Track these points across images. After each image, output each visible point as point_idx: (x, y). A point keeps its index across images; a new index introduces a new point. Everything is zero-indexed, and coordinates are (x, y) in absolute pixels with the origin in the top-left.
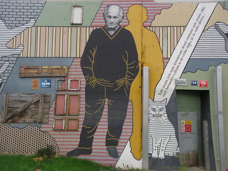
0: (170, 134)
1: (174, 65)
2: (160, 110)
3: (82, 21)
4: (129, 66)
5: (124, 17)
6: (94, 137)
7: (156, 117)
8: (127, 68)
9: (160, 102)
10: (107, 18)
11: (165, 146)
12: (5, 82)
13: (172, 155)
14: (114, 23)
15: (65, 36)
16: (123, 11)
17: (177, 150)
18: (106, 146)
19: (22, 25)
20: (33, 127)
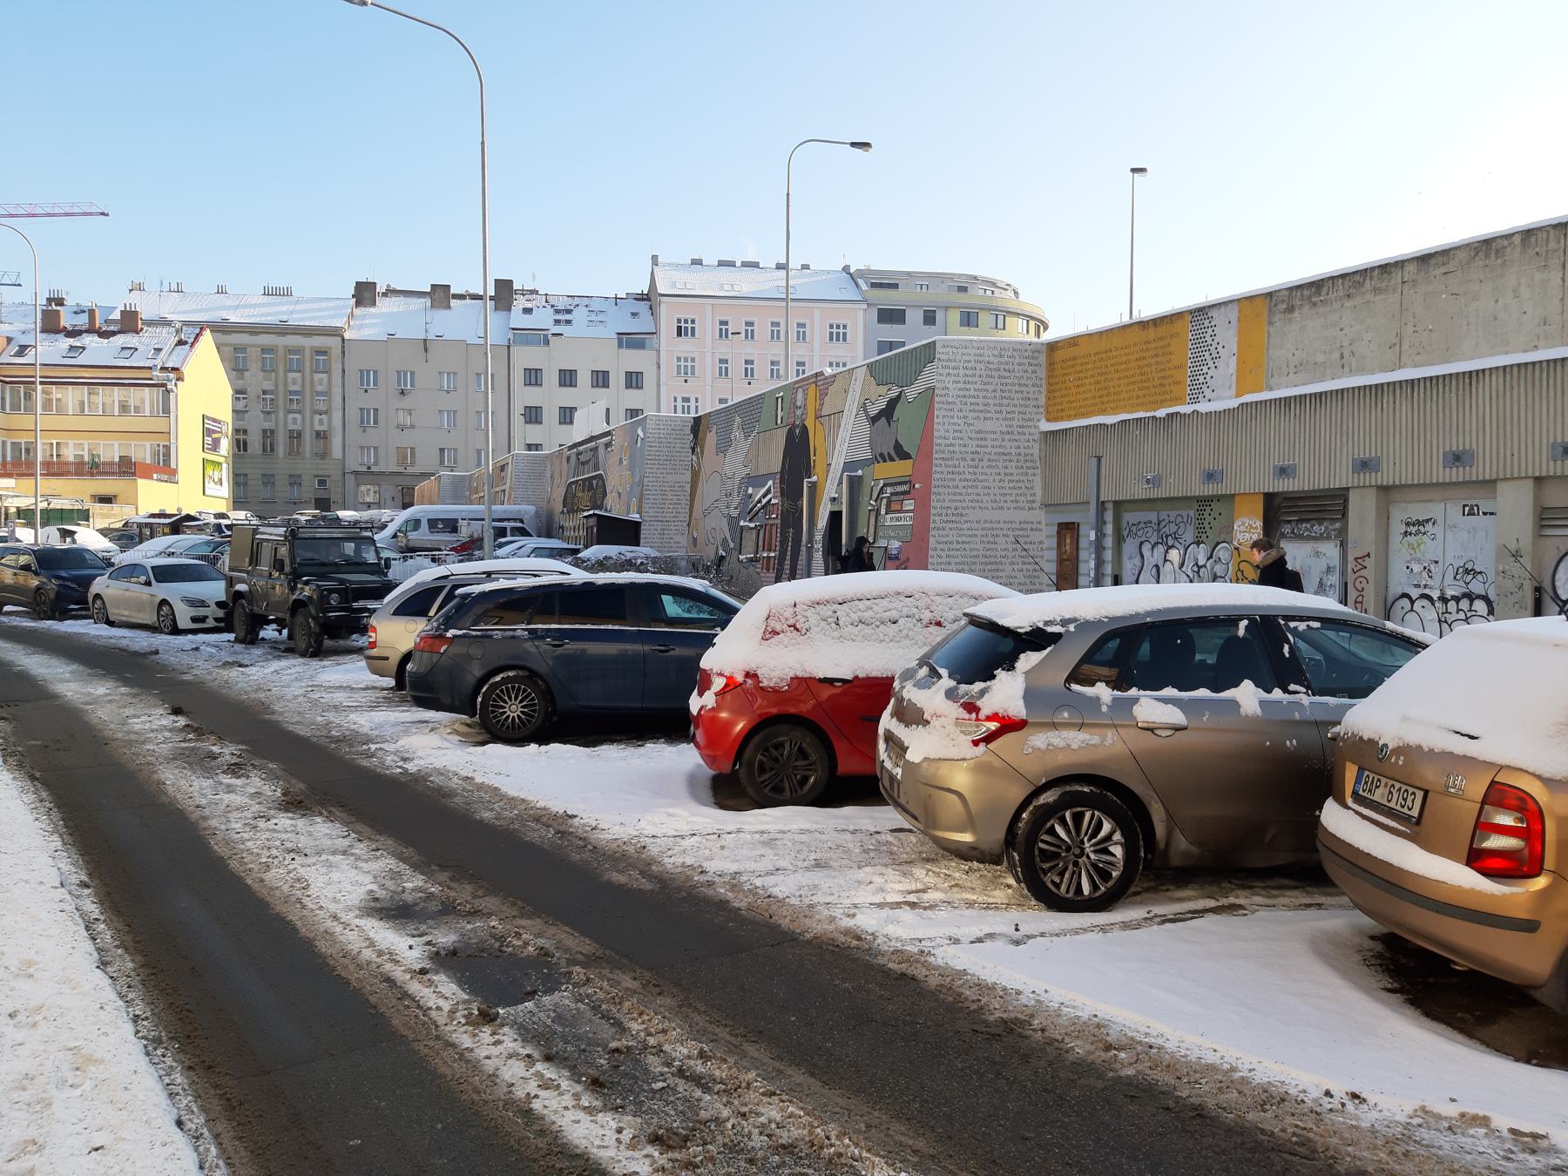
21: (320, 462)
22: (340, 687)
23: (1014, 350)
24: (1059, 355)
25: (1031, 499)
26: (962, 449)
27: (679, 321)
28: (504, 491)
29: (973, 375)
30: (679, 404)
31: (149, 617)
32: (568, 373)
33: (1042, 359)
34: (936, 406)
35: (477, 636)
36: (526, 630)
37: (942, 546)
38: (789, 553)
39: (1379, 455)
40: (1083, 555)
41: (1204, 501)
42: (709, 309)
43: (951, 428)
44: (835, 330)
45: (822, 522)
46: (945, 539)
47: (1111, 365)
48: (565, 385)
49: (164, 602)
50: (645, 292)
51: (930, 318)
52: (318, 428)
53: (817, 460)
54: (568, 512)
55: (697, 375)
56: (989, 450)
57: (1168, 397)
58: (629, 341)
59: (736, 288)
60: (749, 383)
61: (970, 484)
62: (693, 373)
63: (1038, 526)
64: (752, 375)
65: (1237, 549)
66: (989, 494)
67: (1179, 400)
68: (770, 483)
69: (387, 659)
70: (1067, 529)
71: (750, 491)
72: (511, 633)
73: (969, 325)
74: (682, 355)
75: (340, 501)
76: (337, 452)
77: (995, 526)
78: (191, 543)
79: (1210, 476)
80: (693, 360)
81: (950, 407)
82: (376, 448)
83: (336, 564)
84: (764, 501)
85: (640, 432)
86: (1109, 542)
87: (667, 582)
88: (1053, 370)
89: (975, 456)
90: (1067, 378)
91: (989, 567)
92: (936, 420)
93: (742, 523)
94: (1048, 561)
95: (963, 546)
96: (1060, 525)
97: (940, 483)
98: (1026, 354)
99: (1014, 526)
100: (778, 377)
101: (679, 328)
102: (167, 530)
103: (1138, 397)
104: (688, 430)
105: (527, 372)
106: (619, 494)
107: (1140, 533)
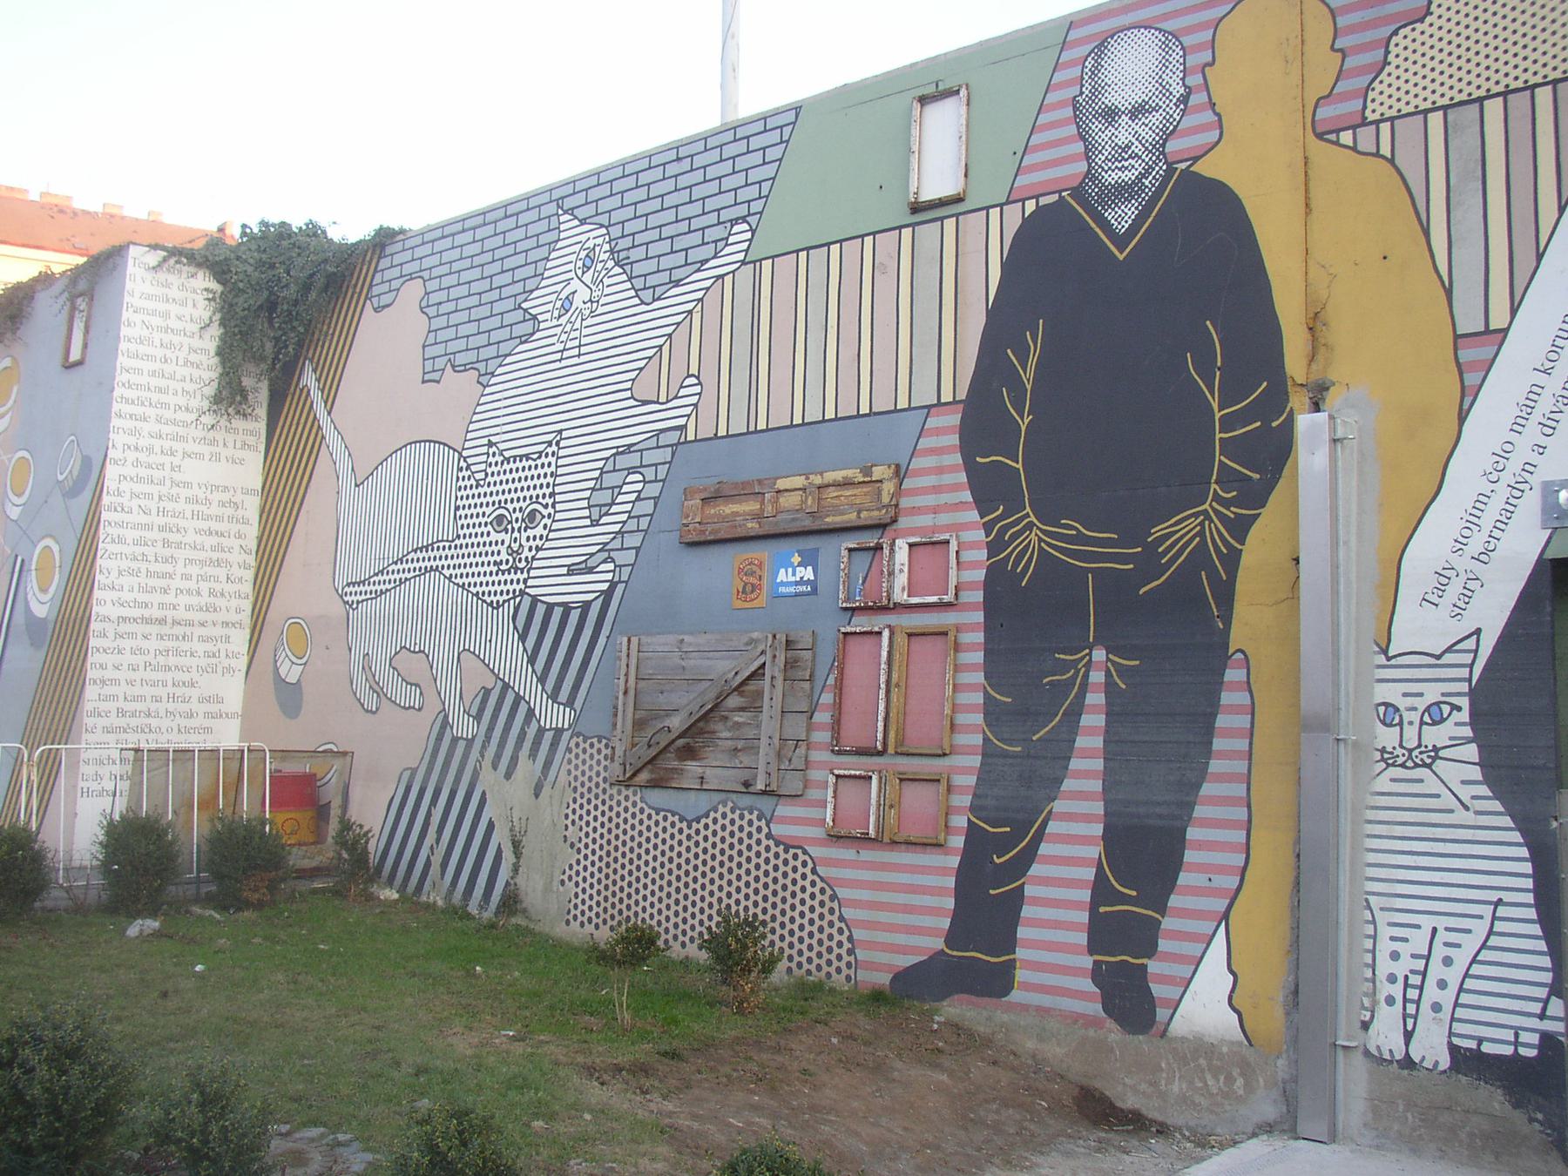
0: (1493, 896)
1: (1541, 379)
2: (1427, 718)
3: (966, 176)
4: (1227, 424)
5: (1189, 94)
6: (1029, 891)
7: (1403, 765)
8: (1218, 436)
9: (1433, 661)
10: (1096, 126)
11: (1453, 976)
12: (625, 578)
13: (1508, 1050)
14: (1137, 148)
15: (885, 284)
16: (1184, 56)
17: (1542, 1016)
18: (1091, 951)
19: (698, 270)
20: (738, 812)
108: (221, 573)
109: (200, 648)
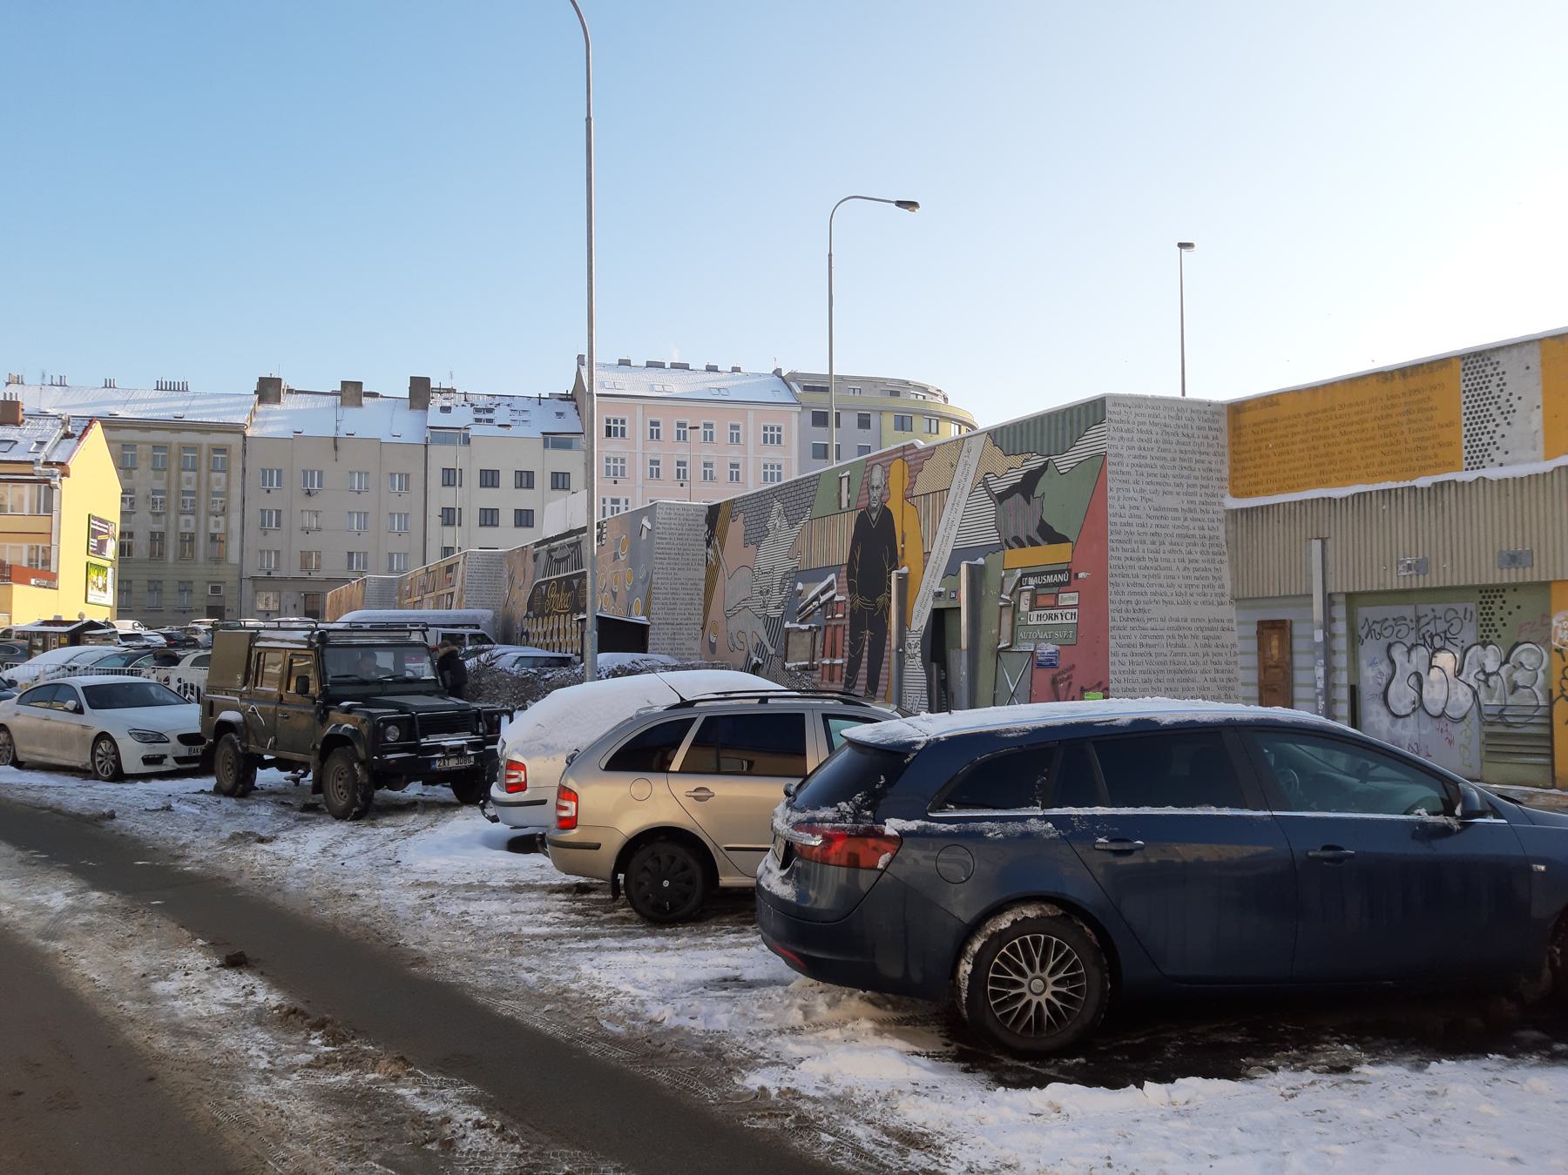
21: (216, 567)
22: (482, 885)
23: (1192, 411)
24: (1247, 418)
25: (1218, 591)
26: (1141, 530)
27: (608, 421)
28: (452, 594)
29: (1149, 441)
30: (608, 505)
31: (80, 757)
32: (489, 474)
33: (1223, 423)
34: (1109, 476)
35: (949, 834)
36: (1046, 818)
37: (1125, 650)
38: (865, 660)
39: (1427, 555)
40: (1300, 660)
41: (1490, 593)
42: (639, 410)
43: (1127, 504)
44: (769, 432)
45: (920, 620)
46: (1127, 641)
47: (1335, 427)
48: (486, 486)
49: (103, 736)
50: (570, 393)
51: (864, 422)
52: (213, 530)
53: (908, 548)
54: (536, 616)
55: (627, 476)
56: (1169, 531)
57: (1431, 462)
58: (554, 441)
59: (667, 388)
60: (682, 485)
61: (1152, 572)
62: (623, 474)
63: (1230, 625)
64: (685, 477)
65: (1559, 651)
66: (1172, 586)
67: (1451, 466)
68: (832, 577)
69: (597, 847)
70: (1280, 628)
71: (800, 586)
72: (1019, 827)
73: (903, 430)
74: (612, 456)
75: (235, 609)
76: (234, 557)
77: (1182, 624)
78: (97, 656)
79: (1513, 559)
80: (623, 461)
81: (1125, 478)
82: (277, 552)
83: (380, 682)
84: (823, 599)
85: (645, 522)
86: (1341, 644)
87: (1187, 717)
88: (1239, 436)
89: (1155, 538)
90: (1263, 444)
91: (1179, 676)
92: (1109, 494)
93: (787, 625)
94: (1242, 668)
95: (1148, 650)
96: (1261, 624)
97: (1118, 572)
98: (1206, 417)
99: (1203, 624)
100: (711, 479)
101: (609, 428)
102: (64, 640)
103: (1381, 464)
104: (702, 520)
105: (446, 472)
106: (614, 594)
107: (1387, 633)
108: (692, 607)
109: (685, 632)
